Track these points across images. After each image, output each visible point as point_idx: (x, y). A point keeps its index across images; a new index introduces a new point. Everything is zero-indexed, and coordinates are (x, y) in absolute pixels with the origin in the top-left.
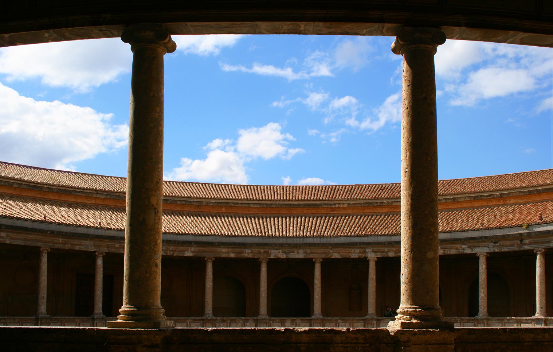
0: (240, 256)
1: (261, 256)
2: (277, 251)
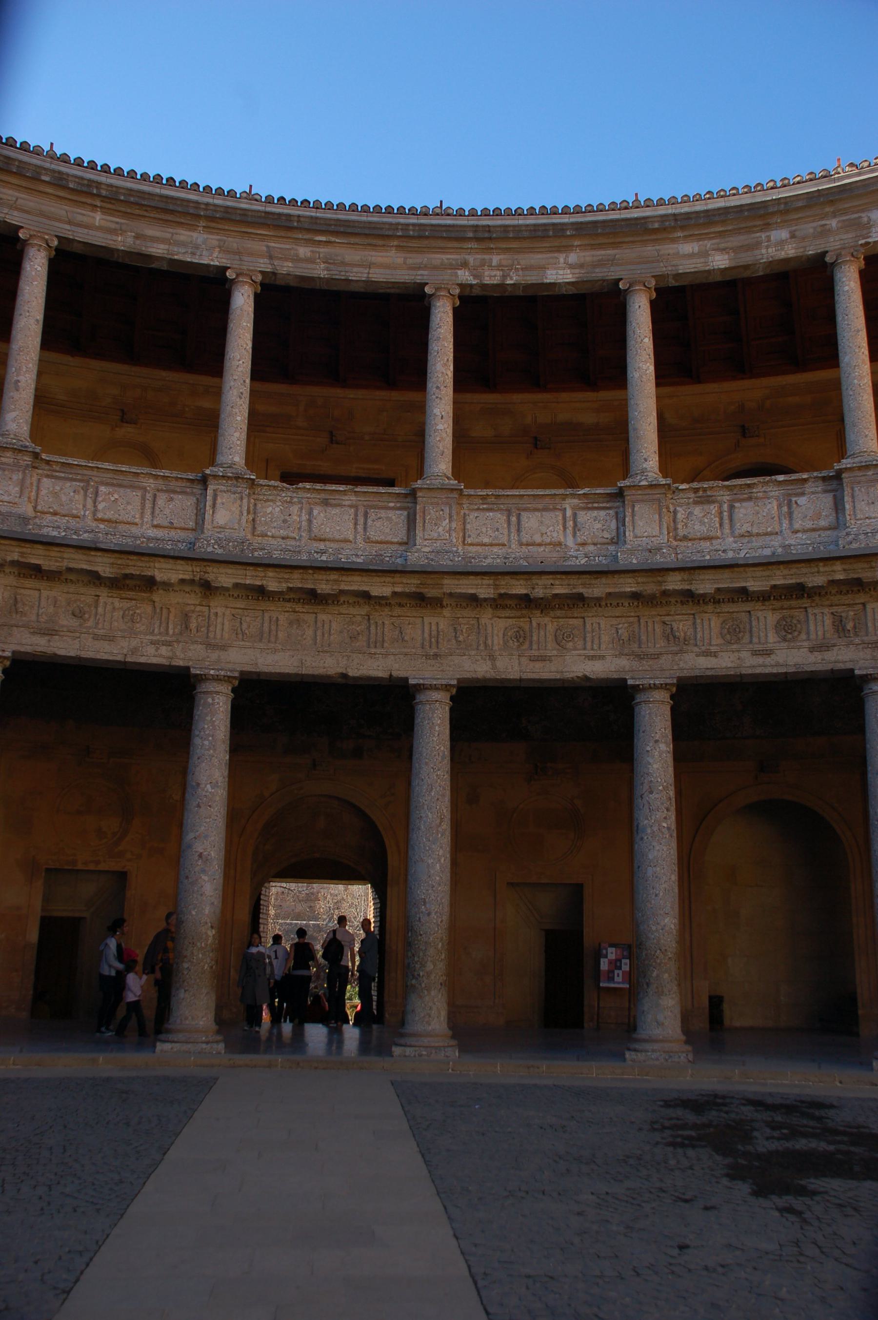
0: (746, 258)
1: (832, 244)
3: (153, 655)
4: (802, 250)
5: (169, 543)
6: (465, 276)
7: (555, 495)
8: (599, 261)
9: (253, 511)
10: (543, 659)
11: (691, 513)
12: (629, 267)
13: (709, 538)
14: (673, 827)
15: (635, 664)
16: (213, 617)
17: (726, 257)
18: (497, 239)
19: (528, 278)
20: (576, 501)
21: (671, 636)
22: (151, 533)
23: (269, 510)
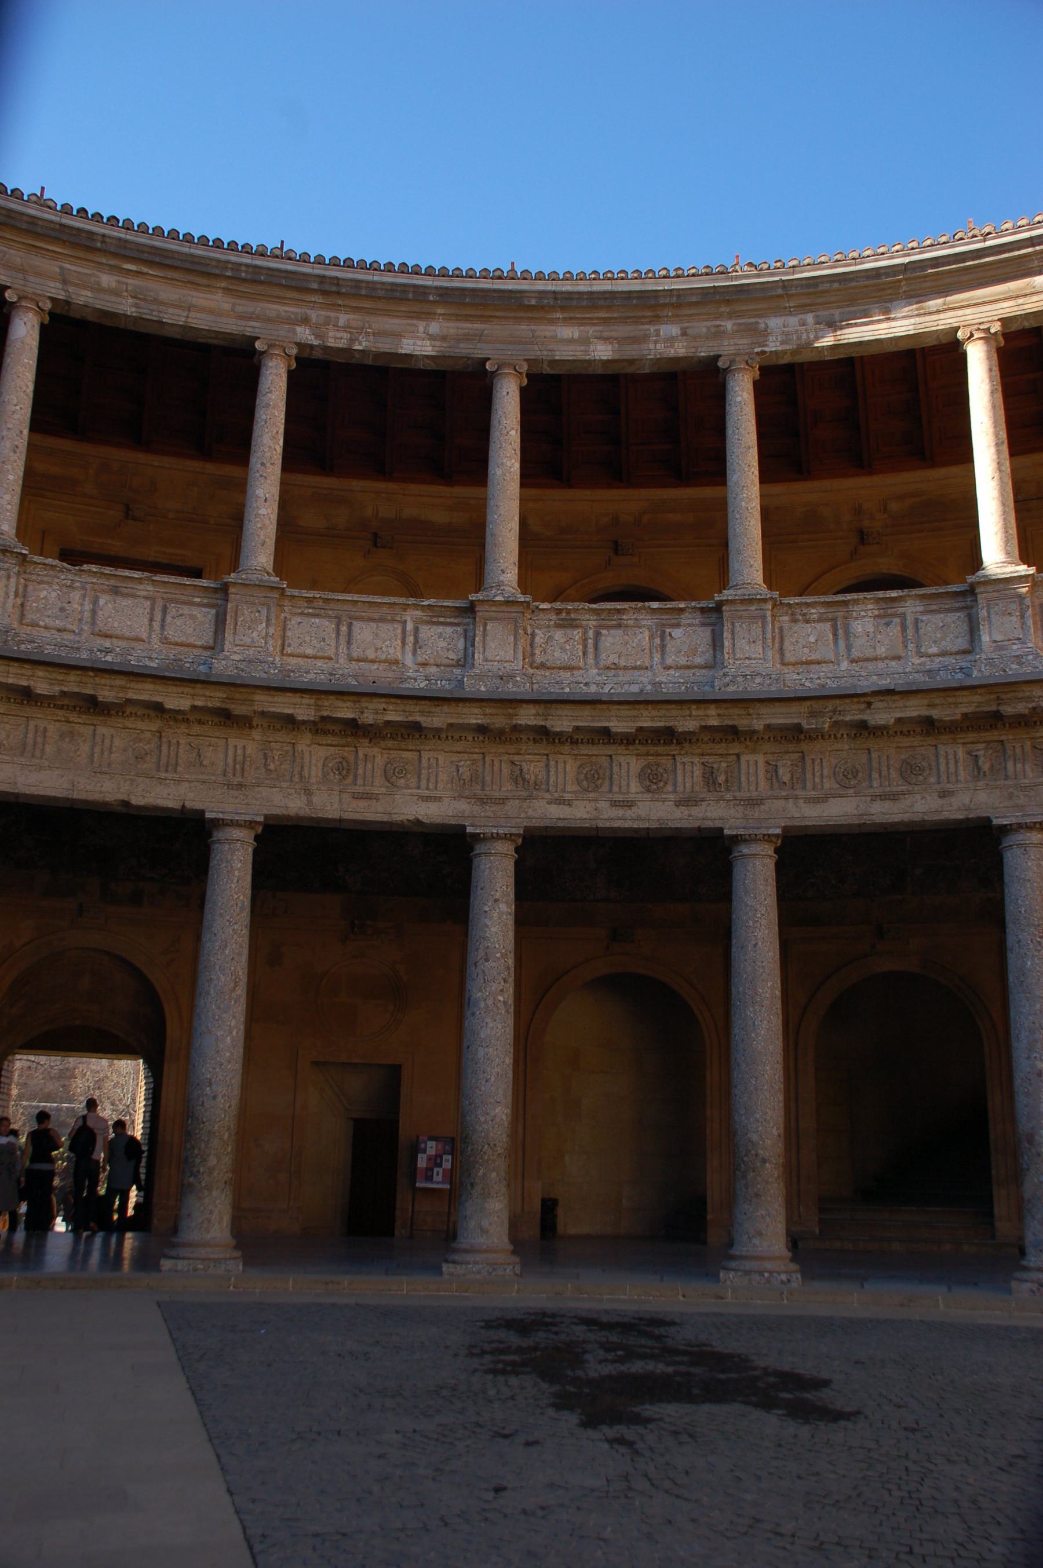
0: (631, 352)
1: (727, 348)
2: (793, 321)
4: (693, 350)
6: (304, 334)
7: (395, 604)
8: (465, 335)
9: (23, 594)
10: (368, 796)
12: (499, 346)
13: (570, 668)
14: (511, 1001)
15: (477, 809)
17: (610, 347)
18: (346, 295)
19: (380, 345)
20: (419, 613)
21: (519, 778)
23: (43, 594)
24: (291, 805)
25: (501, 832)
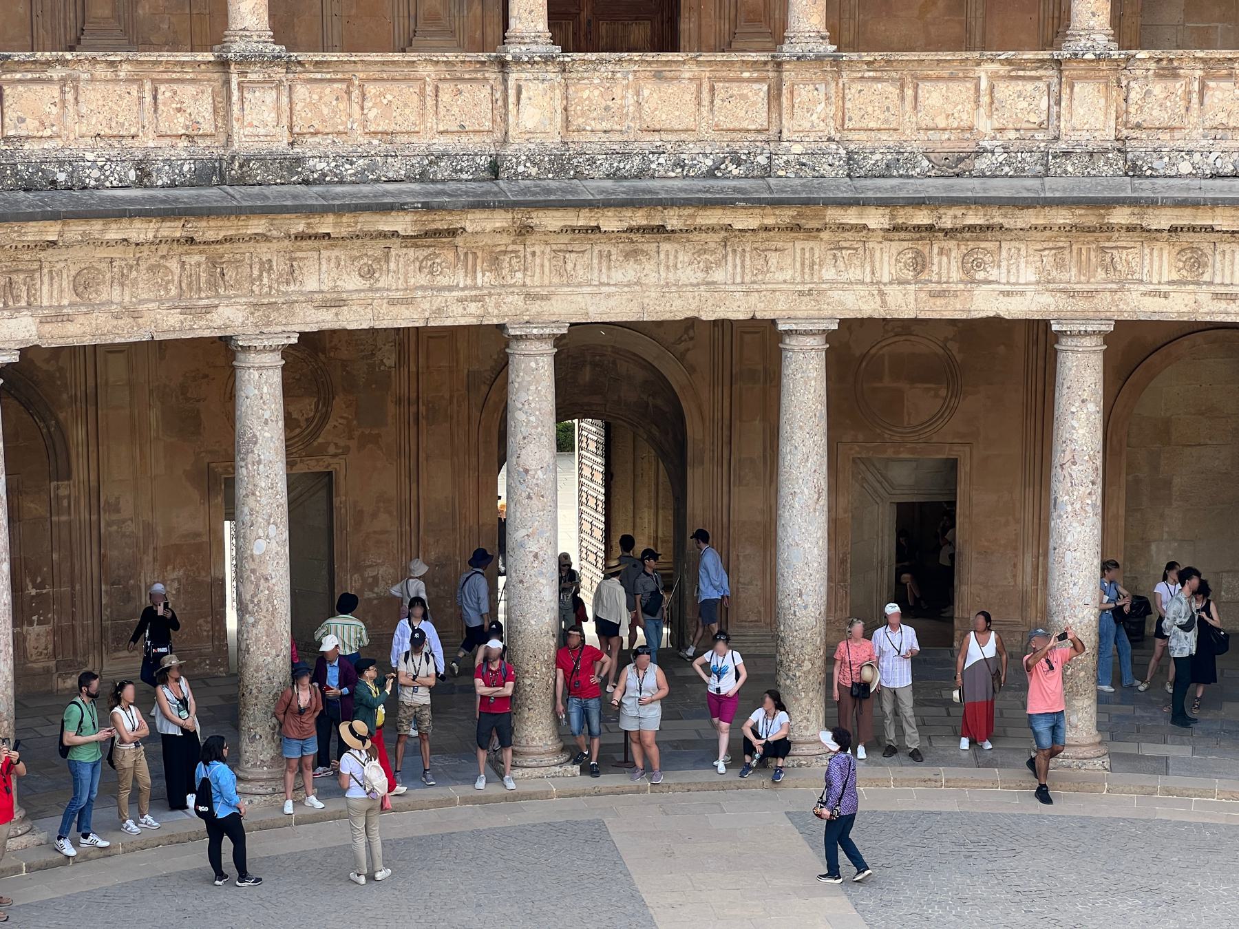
3: (460, 314)
5: (465, 158)
11: (1148, 92)
14: (1099, 503)
16: (529, 257)
22: (442, 143)
23: (586, 94)
24: (864, 307)
25: (1089, 329)
